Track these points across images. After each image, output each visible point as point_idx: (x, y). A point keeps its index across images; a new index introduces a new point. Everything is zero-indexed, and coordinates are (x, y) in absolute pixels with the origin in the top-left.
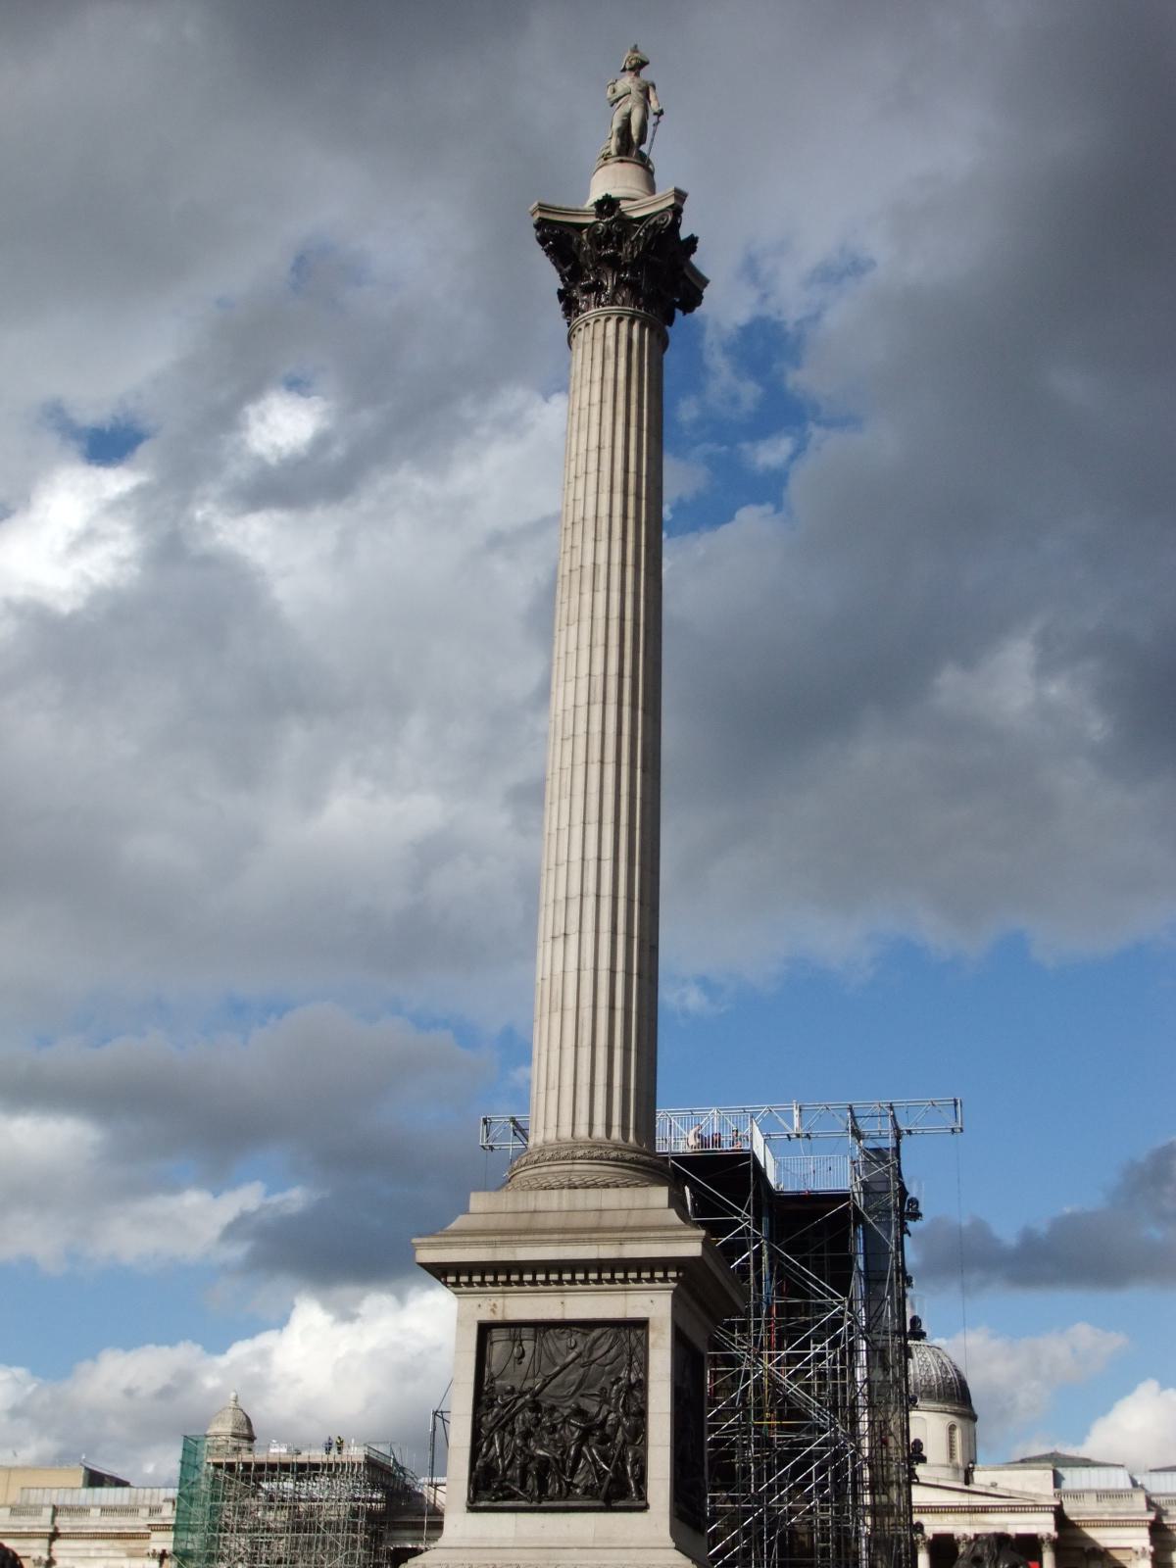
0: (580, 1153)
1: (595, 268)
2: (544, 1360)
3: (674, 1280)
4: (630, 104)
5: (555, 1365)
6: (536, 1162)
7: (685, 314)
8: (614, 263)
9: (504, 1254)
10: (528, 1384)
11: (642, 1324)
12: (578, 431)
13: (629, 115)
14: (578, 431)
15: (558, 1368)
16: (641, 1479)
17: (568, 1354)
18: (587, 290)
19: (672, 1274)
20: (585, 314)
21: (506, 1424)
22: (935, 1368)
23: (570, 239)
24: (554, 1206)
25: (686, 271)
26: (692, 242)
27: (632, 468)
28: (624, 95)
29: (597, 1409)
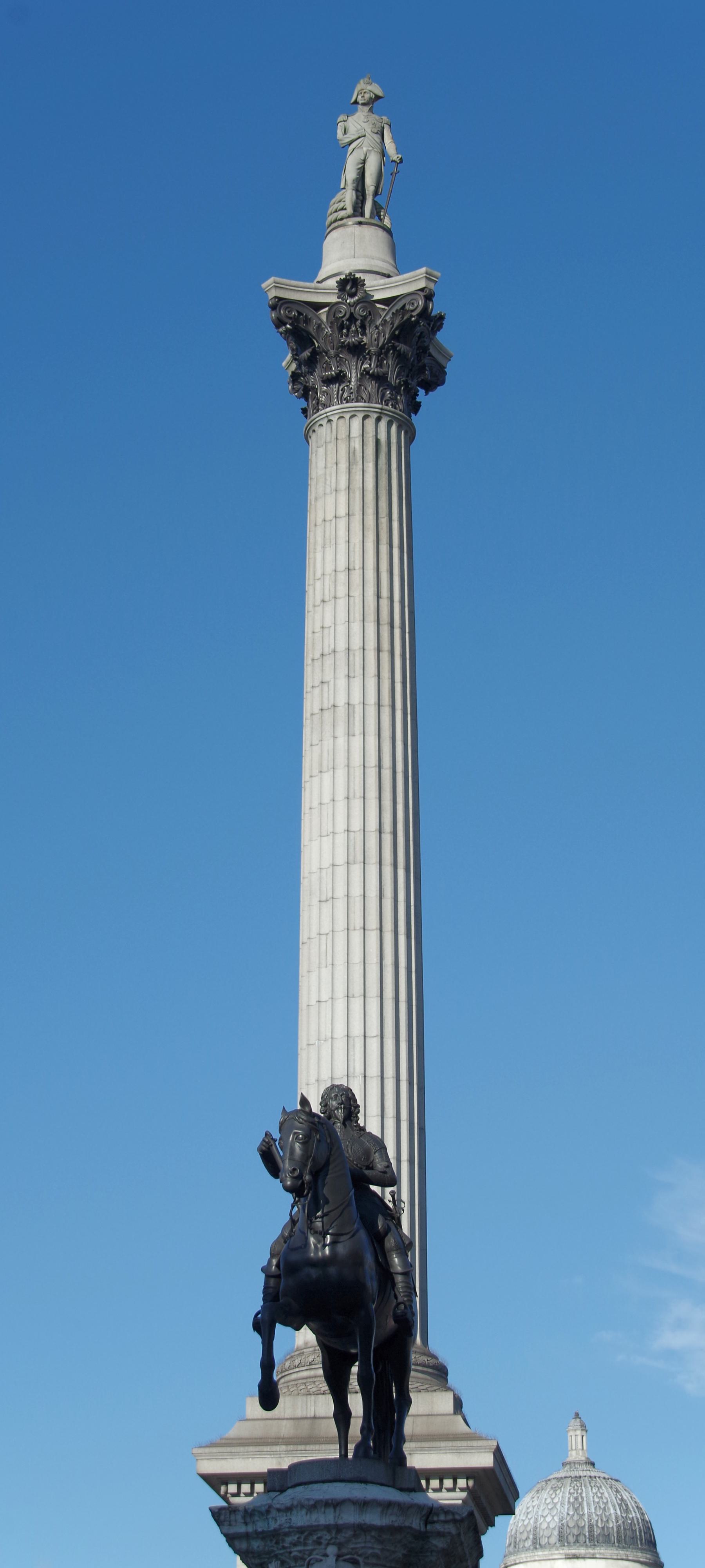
1: (337, 356)
3: (462, 1490)
4: (365, 149)
7: (427, 393)
8: (357, 350)
12: (324, 547)
13: (364, 162)
14: (324, 547)
18: (328, 381)
19: (462, 1483)
22: (614, 1506)
23: (307, 321)
25: (432, 350)
26: (441, 318)
27: (385, 592)
28: (359, 138)
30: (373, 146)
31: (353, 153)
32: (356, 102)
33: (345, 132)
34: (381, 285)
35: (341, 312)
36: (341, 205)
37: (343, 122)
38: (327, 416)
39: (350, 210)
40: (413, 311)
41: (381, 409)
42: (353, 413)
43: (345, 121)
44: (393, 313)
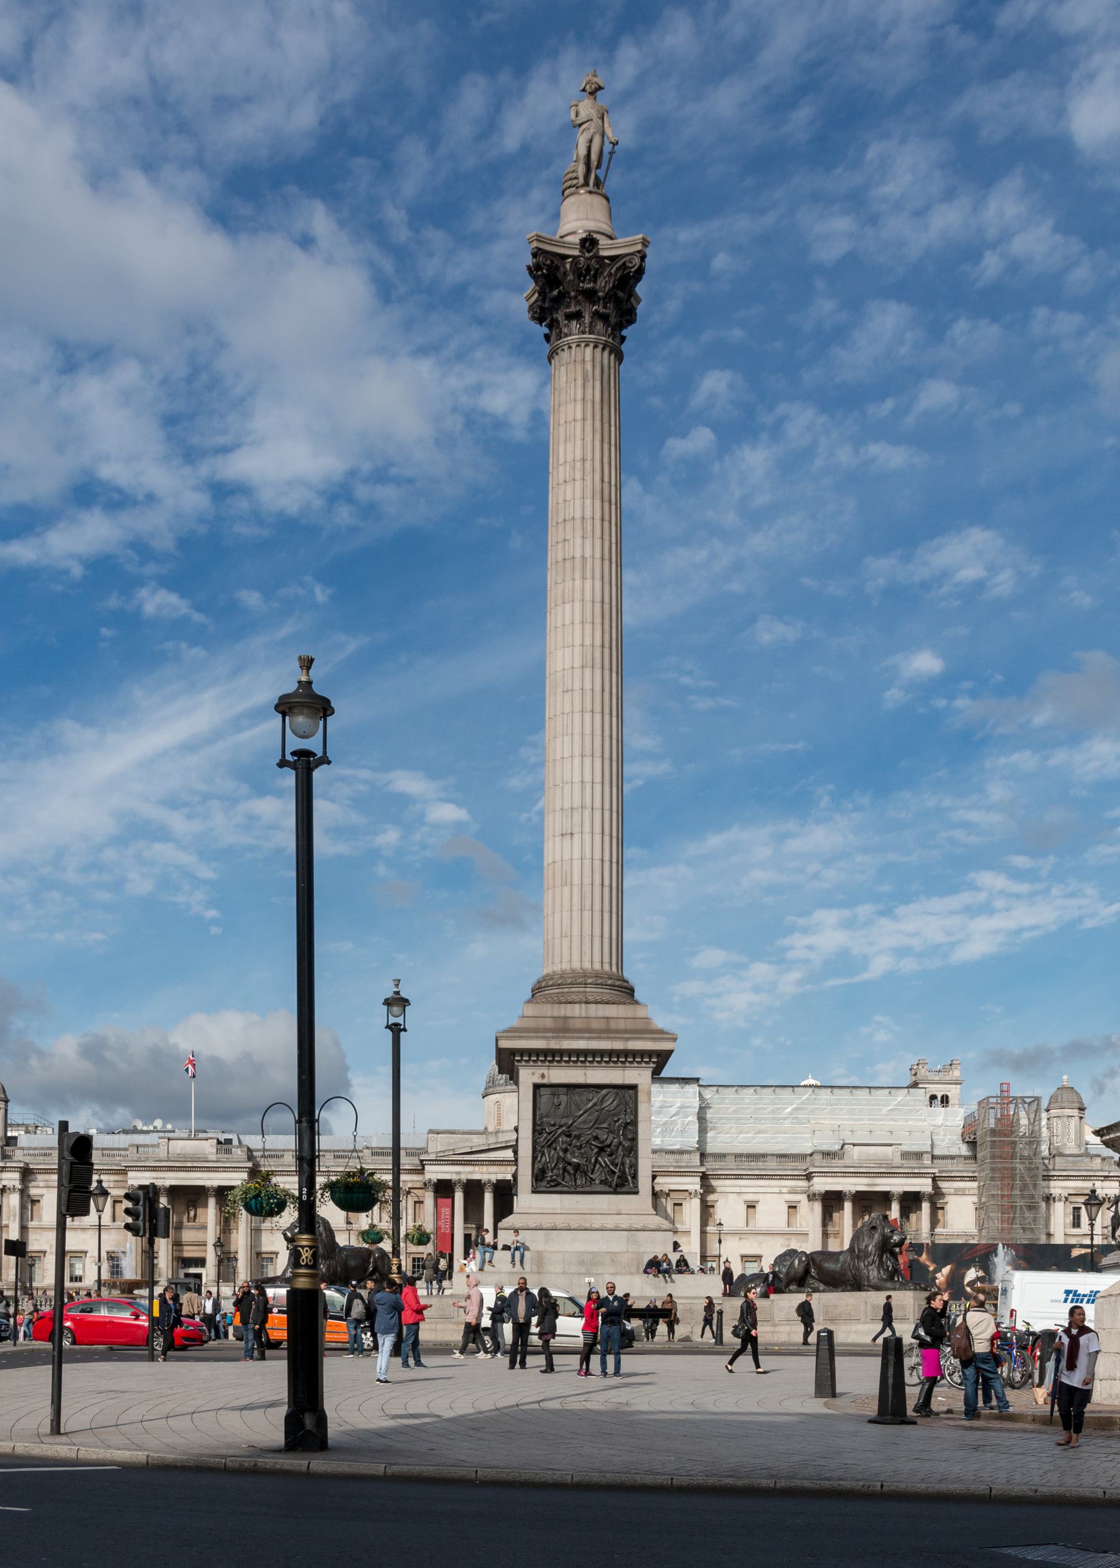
0: (589, 981)
2: (573, 1108)
3: (654, 1062)
5: (580, 1110)
6: (559, 985)
9: (554, 1045)
10: (564, 1121)
11: (634, 1087)
15: (582, 1112)
16: (635, 1177)
17: (588, 1103)
21: (552, 1144)
24: (577, 1014)
29: (606, 1137)
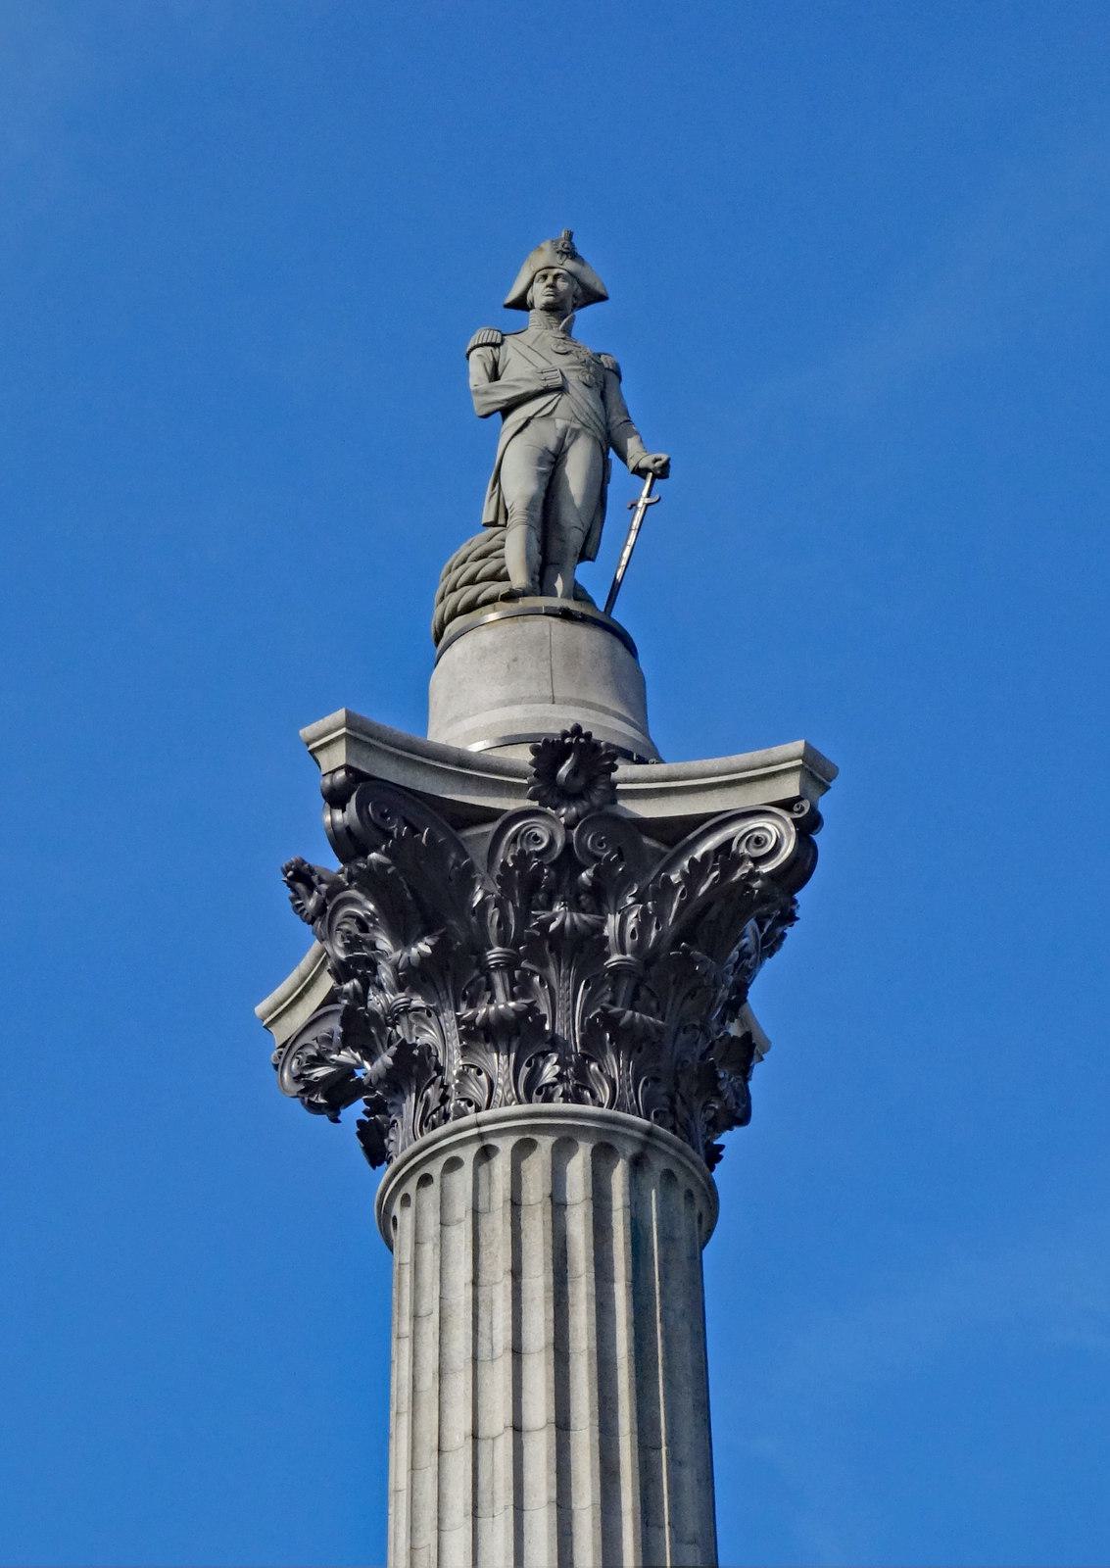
4: (560, 424)
18: (477, 1035)
20: (484, 1115)
30: (582, 419)
31: (526, 430)
32: (522, 304)
33: (495, 375)
34: (657, 780)
35: (536, 838)
36: (491, 566)
37: (491, 348)
38: (481, 1136)
39: (519, 579)
40: (757, 861)
41: (649, 1133)
42: (565, 1133)
43: (496, 345)
44: (693, 861)
